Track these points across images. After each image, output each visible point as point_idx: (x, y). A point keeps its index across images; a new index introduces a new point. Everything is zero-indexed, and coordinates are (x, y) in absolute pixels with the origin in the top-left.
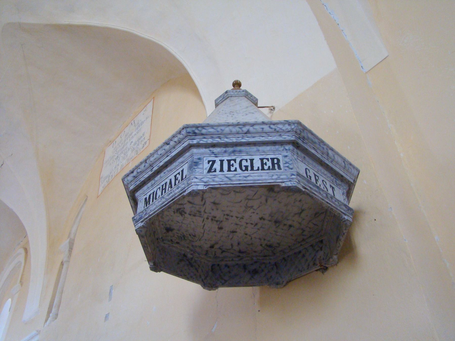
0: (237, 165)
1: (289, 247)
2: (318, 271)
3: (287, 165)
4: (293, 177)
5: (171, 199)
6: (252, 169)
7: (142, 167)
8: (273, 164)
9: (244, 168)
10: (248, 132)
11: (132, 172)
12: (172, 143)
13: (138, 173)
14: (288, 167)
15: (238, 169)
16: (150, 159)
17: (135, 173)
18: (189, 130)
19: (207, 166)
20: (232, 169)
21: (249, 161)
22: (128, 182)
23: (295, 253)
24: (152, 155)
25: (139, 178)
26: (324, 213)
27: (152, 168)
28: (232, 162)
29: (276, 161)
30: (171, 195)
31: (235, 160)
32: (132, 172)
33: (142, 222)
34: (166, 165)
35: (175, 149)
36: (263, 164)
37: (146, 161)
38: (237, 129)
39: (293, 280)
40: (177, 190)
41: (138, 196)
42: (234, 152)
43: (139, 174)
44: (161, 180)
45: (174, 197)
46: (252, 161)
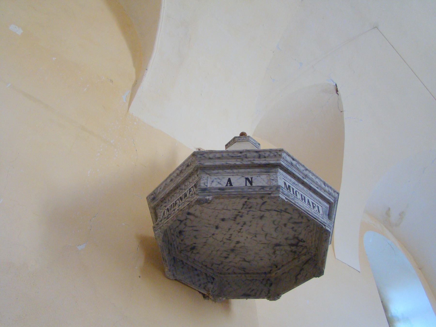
1: (194, 259)
2: (201, 294)
5: (315, 217)
7: (302, 168)
12: (327, 188)
13: (296, 166)
16: (309, 173)
17: (294, 162)
22: (285, 158)
23: (192, 267)
24: (313, 174)
25: (292, 167)
26: (244, 272)
27: (305, 177)
30: (316, 215)
32: (293, 159)
33: (286, 198)
34: (310, 188)
35: (324, 192)
37: (307, 170)
39: (182, 283)
40: (321, 218)
41: (280, 173)
43: (295, 166)
44: (301, 190)
45: (317, 218)
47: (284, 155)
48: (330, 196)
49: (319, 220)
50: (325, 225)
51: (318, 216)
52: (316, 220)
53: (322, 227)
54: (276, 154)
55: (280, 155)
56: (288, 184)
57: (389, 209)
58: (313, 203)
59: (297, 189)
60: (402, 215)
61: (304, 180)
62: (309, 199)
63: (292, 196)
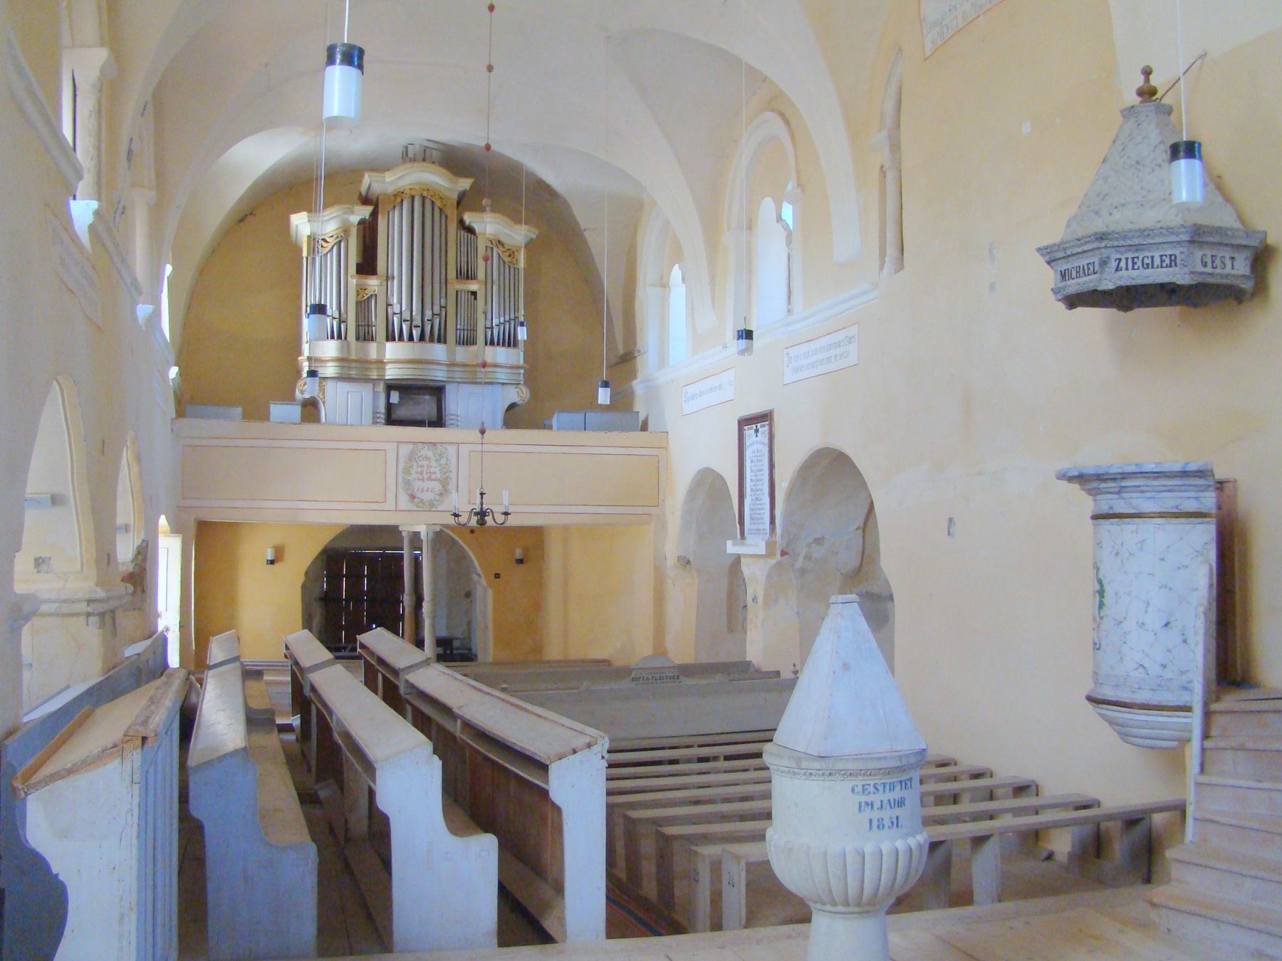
0: (1139, 263)
3: (1182, 262)
4: (1186, 276)
6: (1153, 267)
8: (1171, 260)
9: (1145, 266)
10: (1149, 235)
11: (1047, 249)
14: (1183, 264)
15: (1141, 267)
18: (1097, 236)
19: (1114, 264)
20: (1136, 267)
21: (1150, 258)
28: (1136, 260)
29: (1173, 257)
31: (1138, 258)
36: (1162, 261)
38: (1138, 234)
42: (1137, 250)
46: (1152, 257)
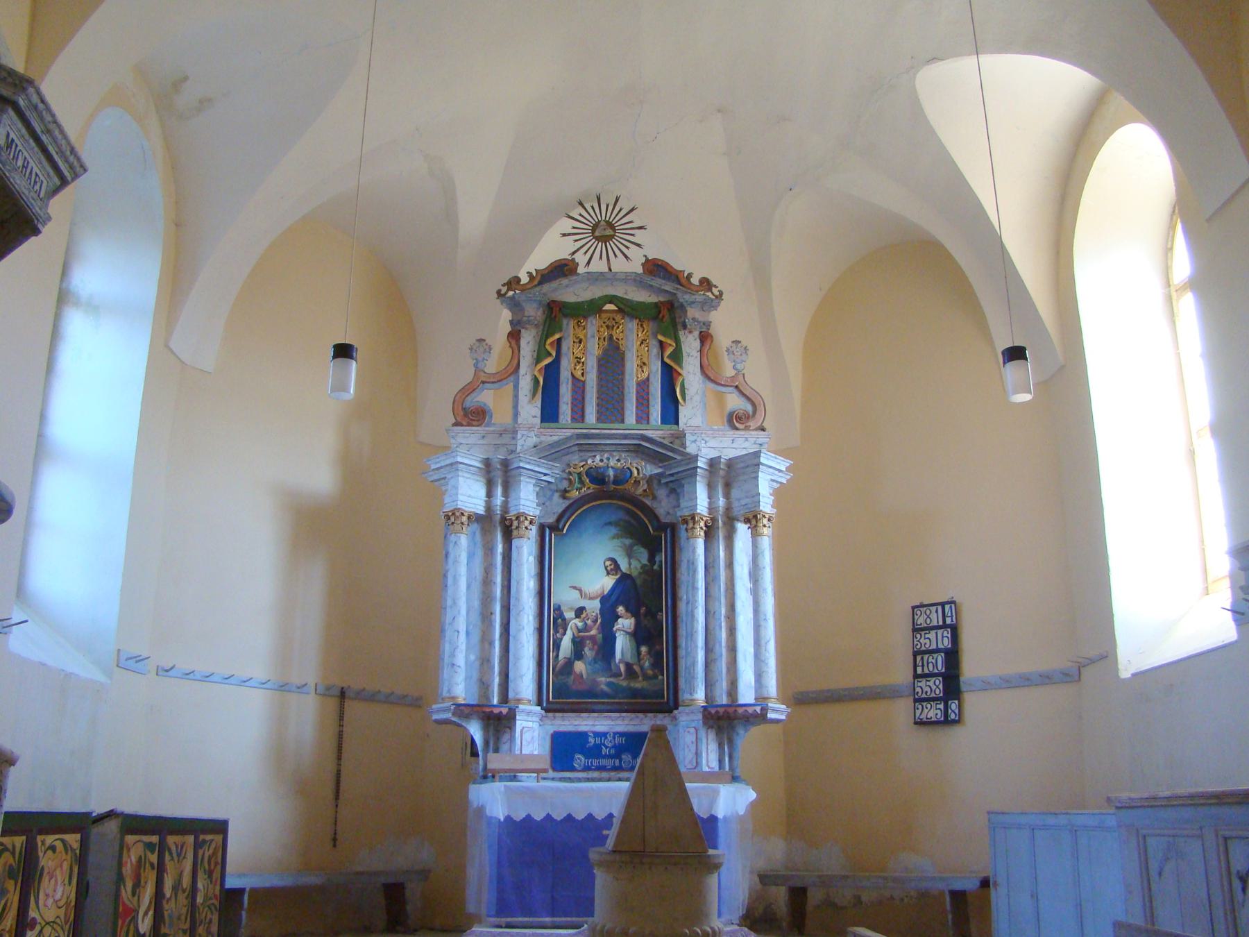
7: (49, 118)
12: (71, 158)
17: (41, 106)
24: (62, 131)
30: (33, 202)
34: (45, 150)
37: (55, 122)
40: (37, 209)
41: (9, 114)
45: (31, 207)
47: (31, 90)
48: (70, 170)
49: (34, 211)
50: (37, 219)
51: (35, 204)
52: (28, 209)
53: (33, 221)
54: (17, 82)
55: (24, 88)
56: (12, 135)
57: (186, 79)
58: (37, 175)
59: (24, 147)
60: (204, 103)
61: (42, 137)
62: (34, 166)
63: (10, 166)
